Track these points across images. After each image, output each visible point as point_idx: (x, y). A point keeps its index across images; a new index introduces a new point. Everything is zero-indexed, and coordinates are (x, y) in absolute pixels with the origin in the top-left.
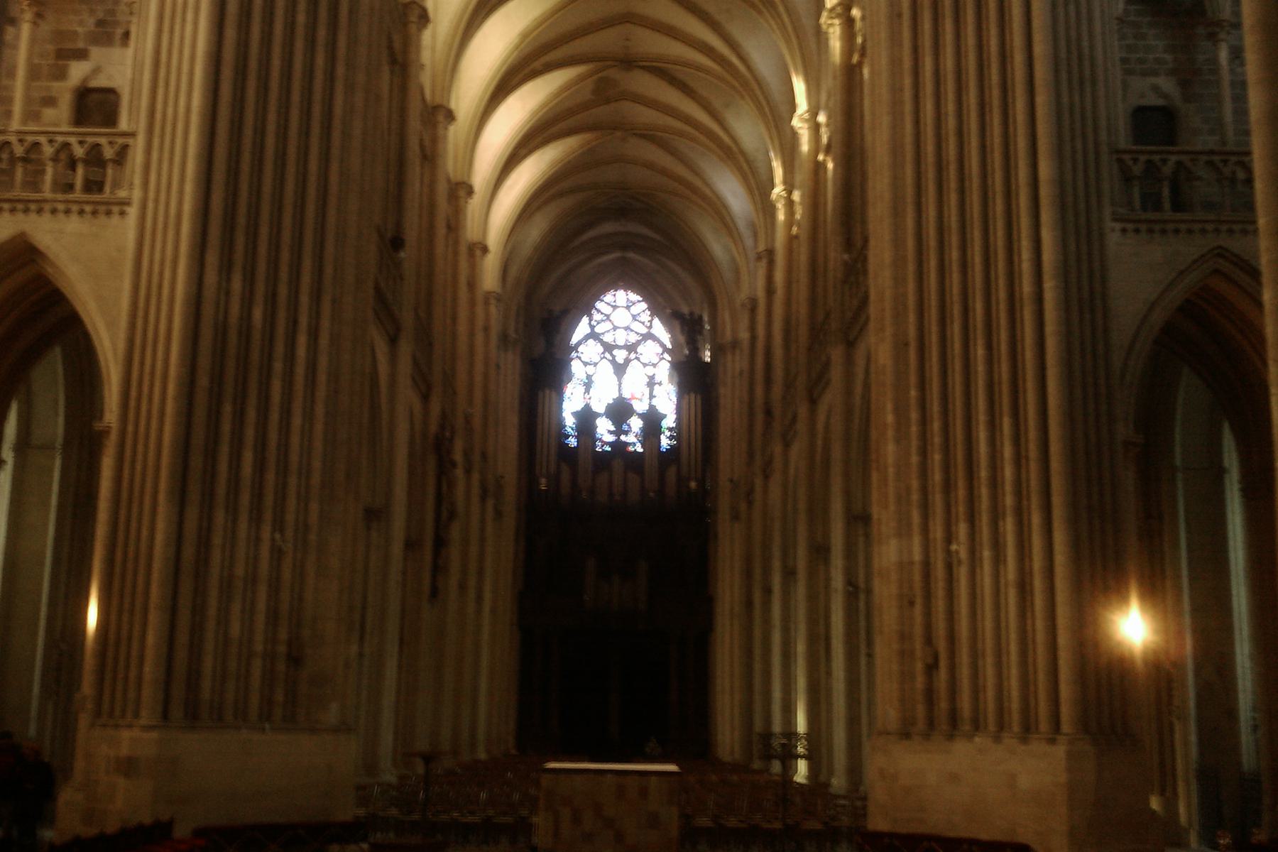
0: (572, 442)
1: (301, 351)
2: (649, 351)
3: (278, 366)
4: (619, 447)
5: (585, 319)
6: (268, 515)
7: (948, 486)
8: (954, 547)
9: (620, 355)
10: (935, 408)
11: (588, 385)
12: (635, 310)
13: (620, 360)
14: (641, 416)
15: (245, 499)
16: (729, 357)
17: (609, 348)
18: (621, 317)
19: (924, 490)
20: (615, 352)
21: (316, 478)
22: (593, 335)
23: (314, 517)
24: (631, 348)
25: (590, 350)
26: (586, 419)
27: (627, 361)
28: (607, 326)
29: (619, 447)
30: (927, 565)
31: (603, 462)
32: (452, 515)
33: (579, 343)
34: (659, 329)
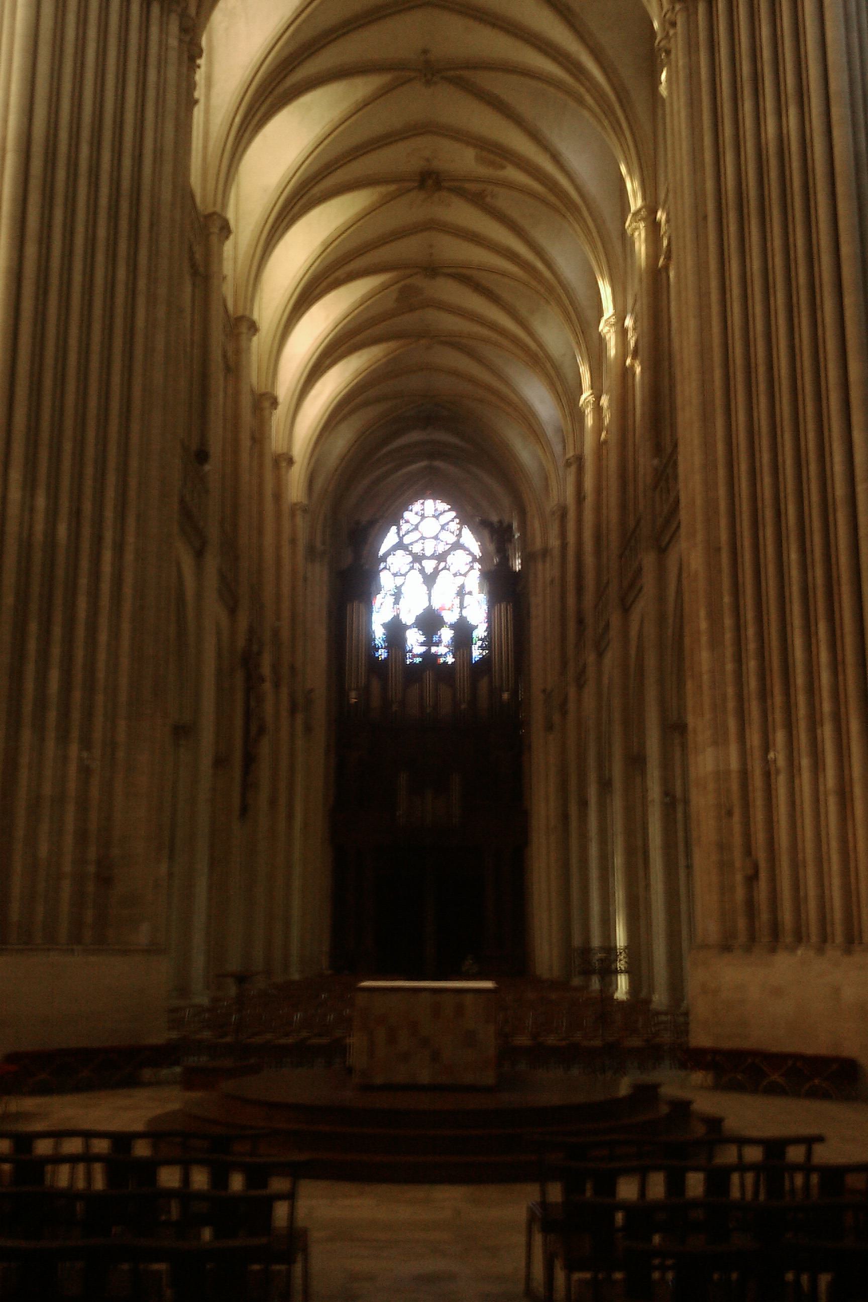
0: (382, 654)
1: (107, 568)
2: (459, 560)
3: (83, 581)
4: (429, 659)
5: (394, 529)
6: (75, 733)
7: (764, 694)
8: (771, 755)
9: (429, 566)
10: (750, 615)
11: (397, 595)
14: (452, 627)
15: (52, 716)
16: (540, 567)
17: (418, 558)
18: (430, 527)
19: (740, 698)
20: (425, 563)
21: (123, 697)
22: (400, 546)
23: (121, 736)
24: (441, 557)
25: (399, 561)
26: (396, 630)
27: (436, 572)
29: (429, 659)
30: (744, 774)
31: (414, 674)
32: (262, 730)
33: (388, 554)
34: (469, 539)
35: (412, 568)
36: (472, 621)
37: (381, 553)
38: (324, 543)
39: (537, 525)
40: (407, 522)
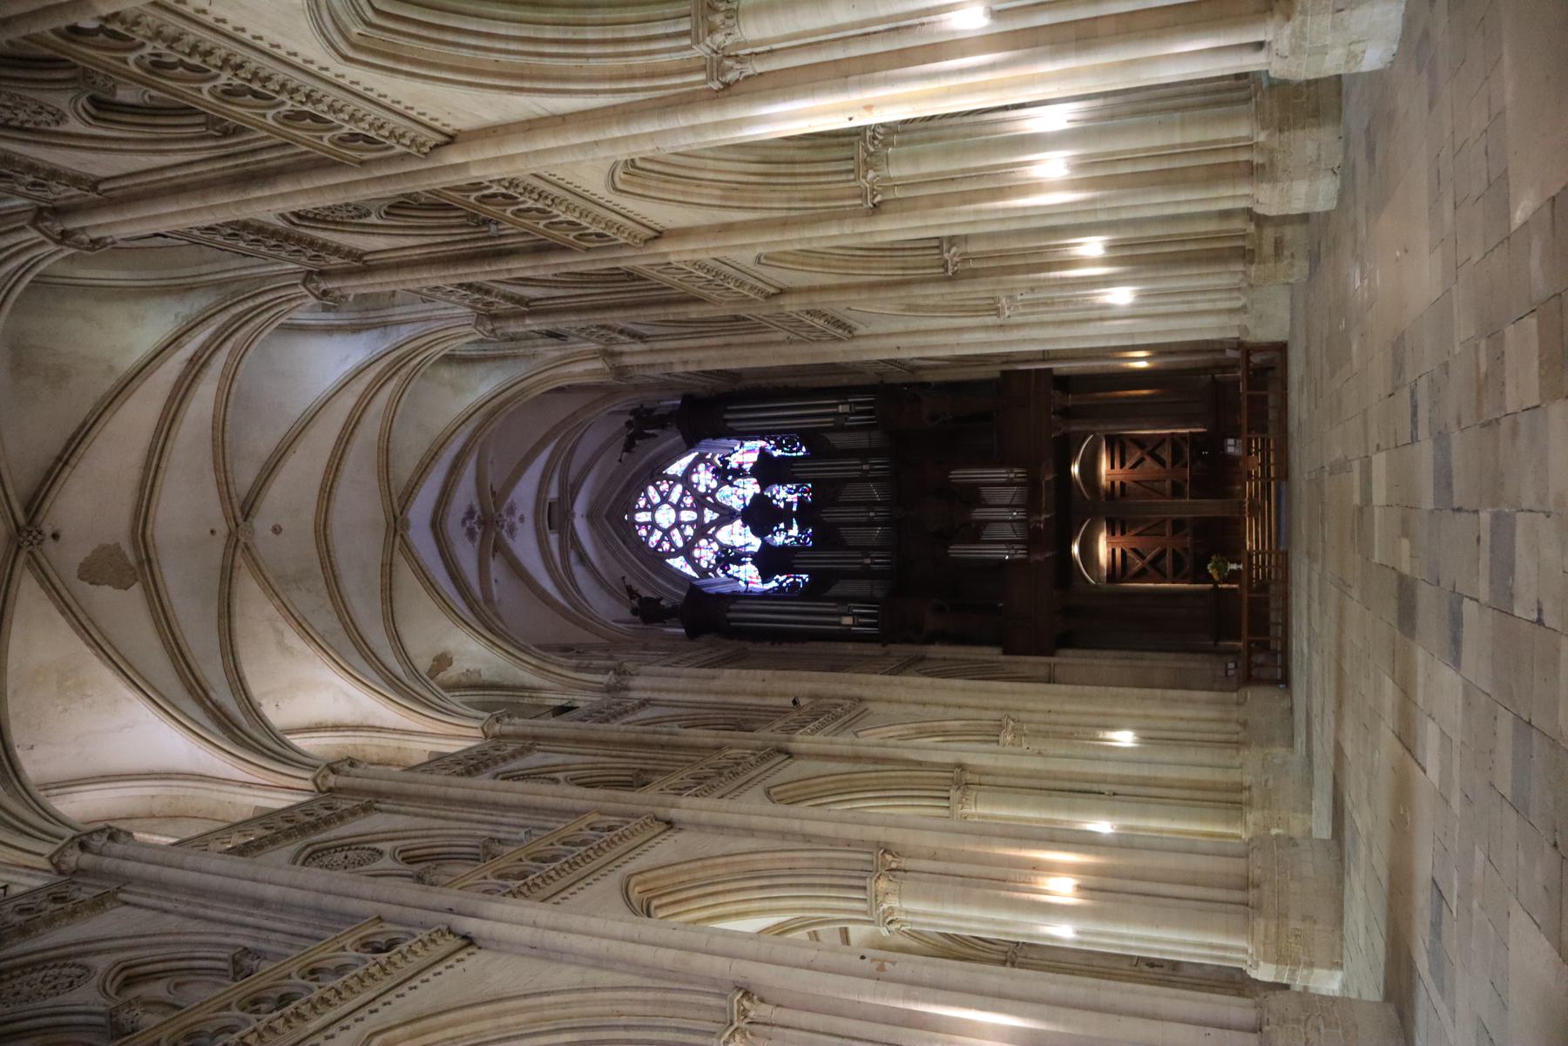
4: (805, 515)
12: (657, 499)
13: (716, 516)
14: (764, 484)
16: (627, 360)
17: (702, 530)
18: (665, 516)
20: (707, 520)
22: (687, 551)
24: (701, 502)
26: (768, 561)
27: (717, 507)
28: (676, 536)
29: (805, 515)
31: (826, 537)
33: (696, 567)
34: (677, 468)
35: (713, 537)
36: (754, 457)
37: (695, 575)
38: (606, 670)
39: (579, 368)
40: (659, 543)
